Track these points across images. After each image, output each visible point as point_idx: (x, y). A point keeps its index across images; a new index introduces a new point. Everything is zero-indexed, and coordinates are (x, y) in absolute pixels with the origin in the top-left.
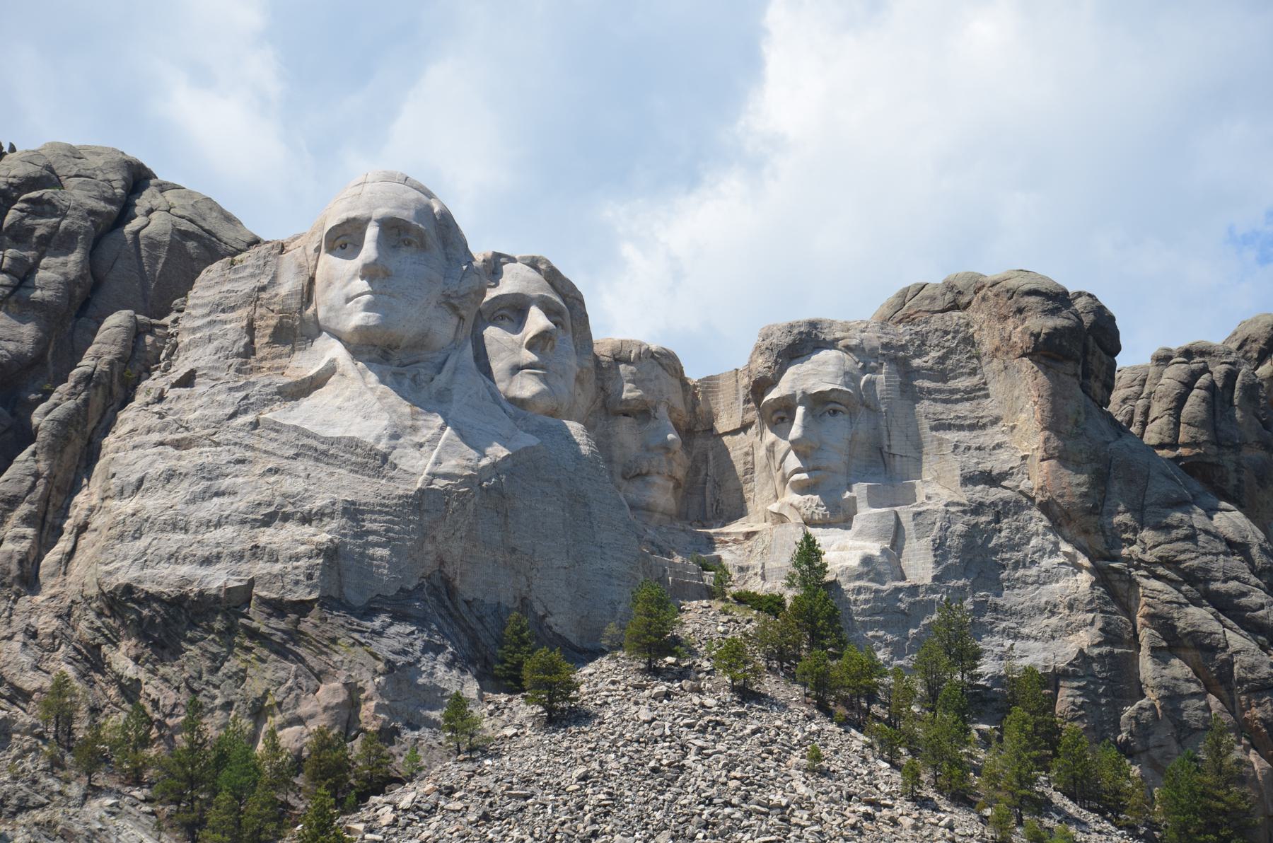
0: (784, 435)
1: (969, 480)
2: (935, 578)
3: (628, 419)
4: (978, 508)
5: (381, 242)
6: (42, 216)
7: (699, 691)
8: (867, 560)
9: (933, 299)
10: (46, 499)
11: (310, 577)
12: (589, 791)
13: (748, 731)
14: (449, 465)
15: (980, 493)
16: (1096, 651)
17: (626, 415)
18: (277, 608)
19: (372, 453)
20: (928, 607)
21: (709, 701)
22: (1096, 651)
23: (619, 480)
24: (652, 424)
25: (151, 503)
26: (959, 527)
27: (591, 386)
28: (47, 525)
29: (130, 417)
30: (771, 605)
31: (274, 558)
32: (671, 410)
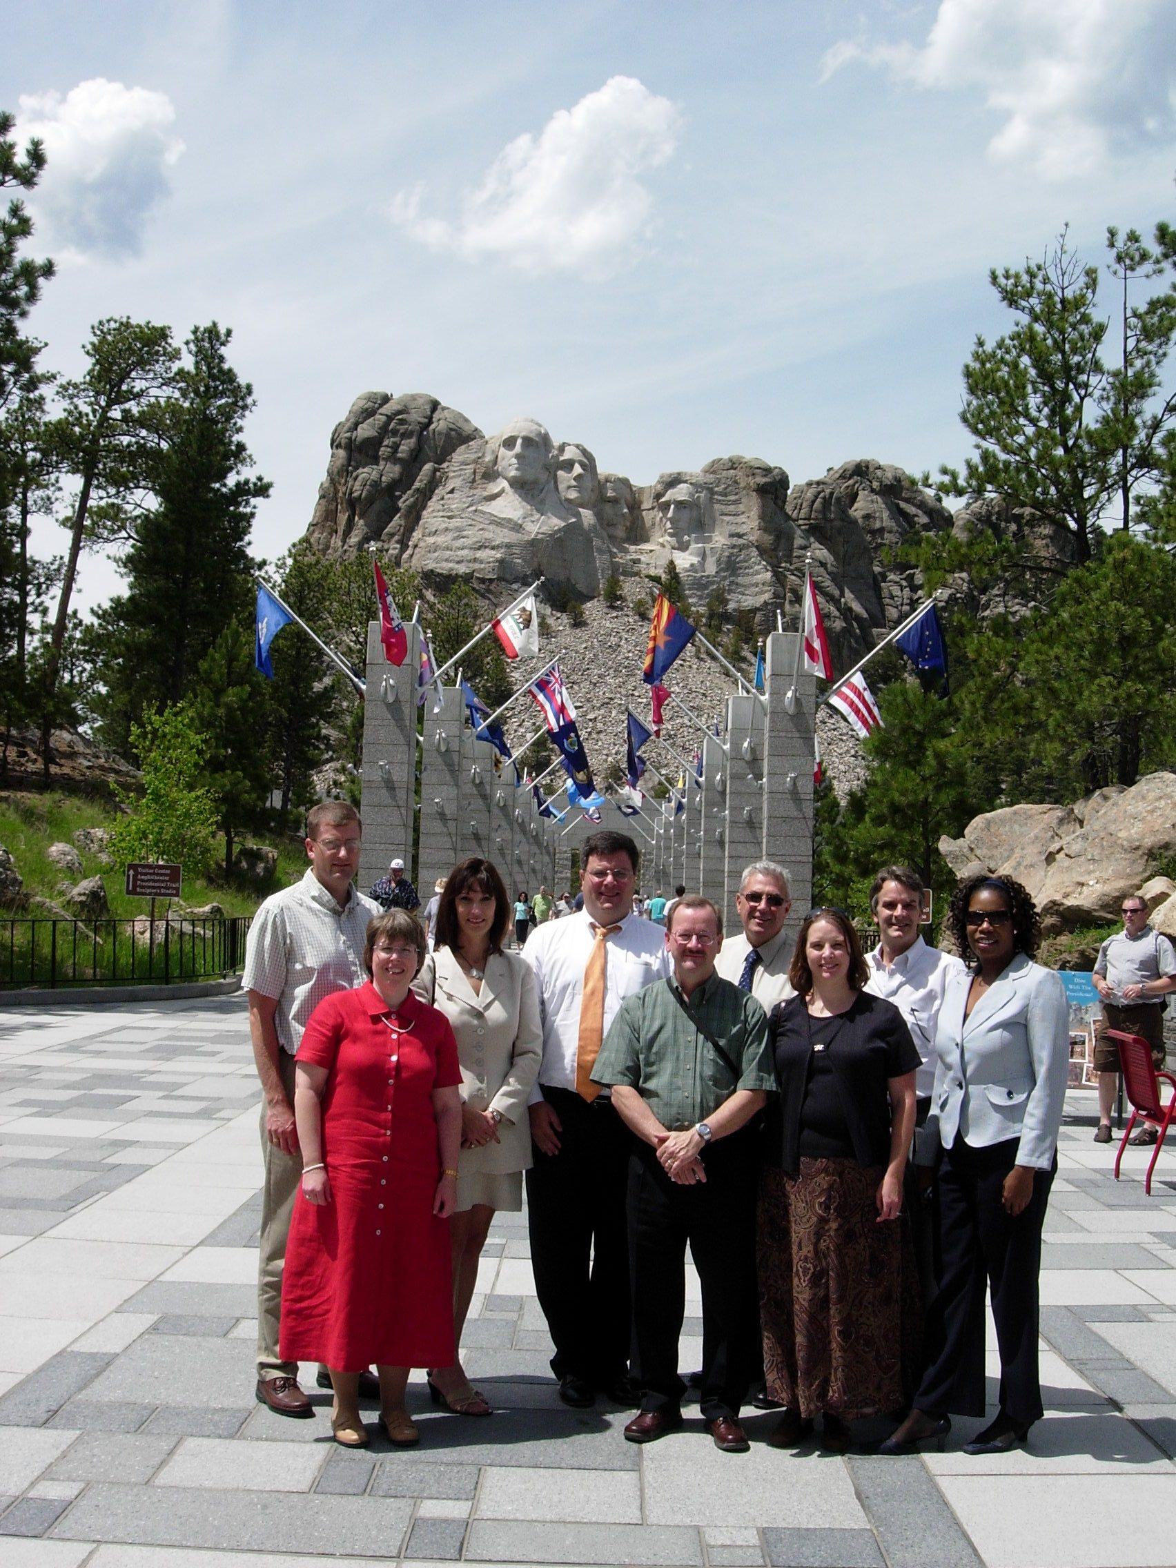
0: (665, 514)
1: (732, 536)
4: (734, 547)
5: (523, 445)
8: (692, 565)
10: (404, 534)
14: (543, 530)
15: (735, 540)
18: (482, 580)
19: (516, 524)
20: (713, 583)
25: (440, 539)
26: (726, 554)
27: (597, 492)
28: (404, 545)
29: (433, 504)
30: (656, 579)
31: (481, 562)
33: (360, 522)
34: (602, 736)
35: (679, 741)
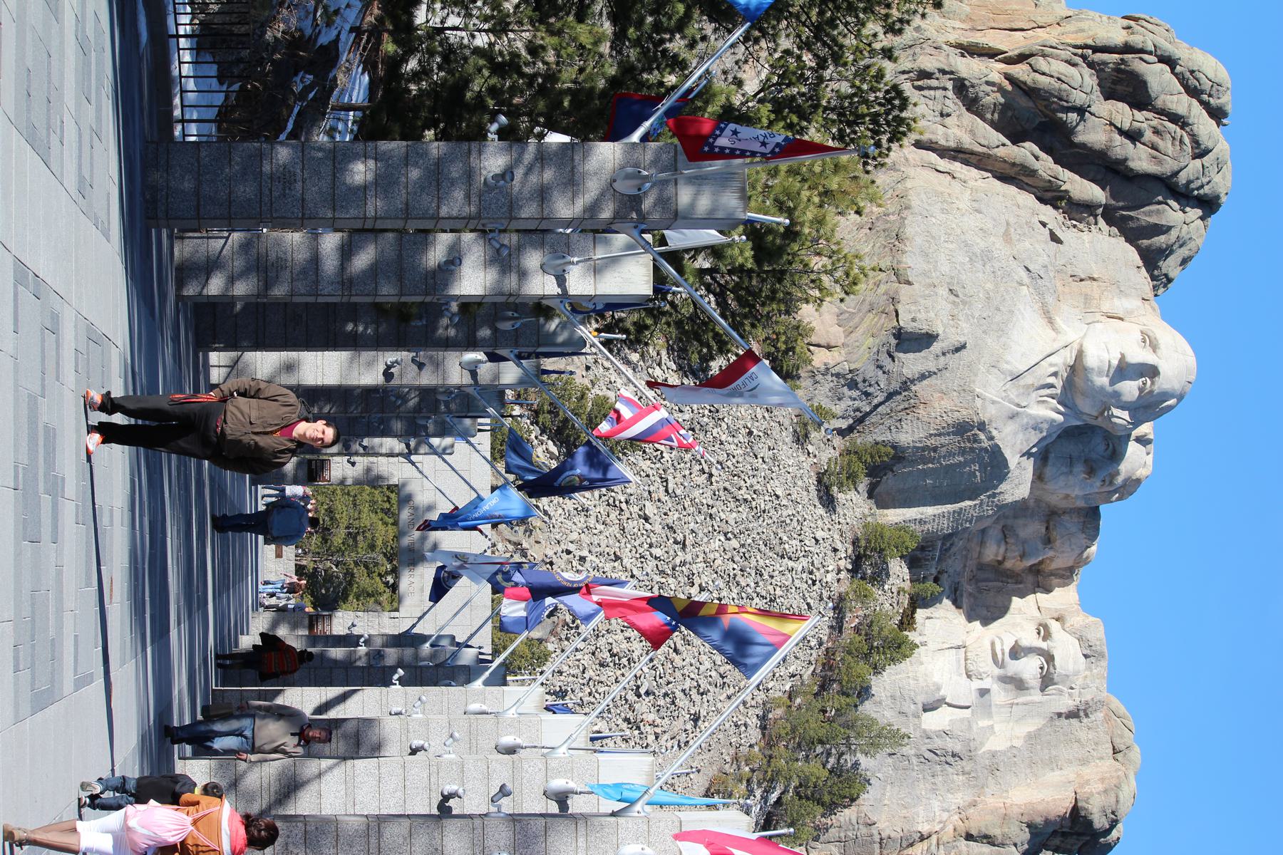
2: (925, 731)
3: (1043, 530)
6: (1173, 144)
7: (839, 571)
9: (1122, 737)
11: (914, 320)
12: (767, 498)
13: (809, 600)
16: (875, 832)
17: (1047, 528)
21: (830, 577)
22: (875, 832)
23: (1002, 523)
24: (1040, 546)
26: (958, 748)
27: (1064, 504)
32: (1051, 559)
33: (995, 71)
34: (615, 530)
35: (610, 672)
